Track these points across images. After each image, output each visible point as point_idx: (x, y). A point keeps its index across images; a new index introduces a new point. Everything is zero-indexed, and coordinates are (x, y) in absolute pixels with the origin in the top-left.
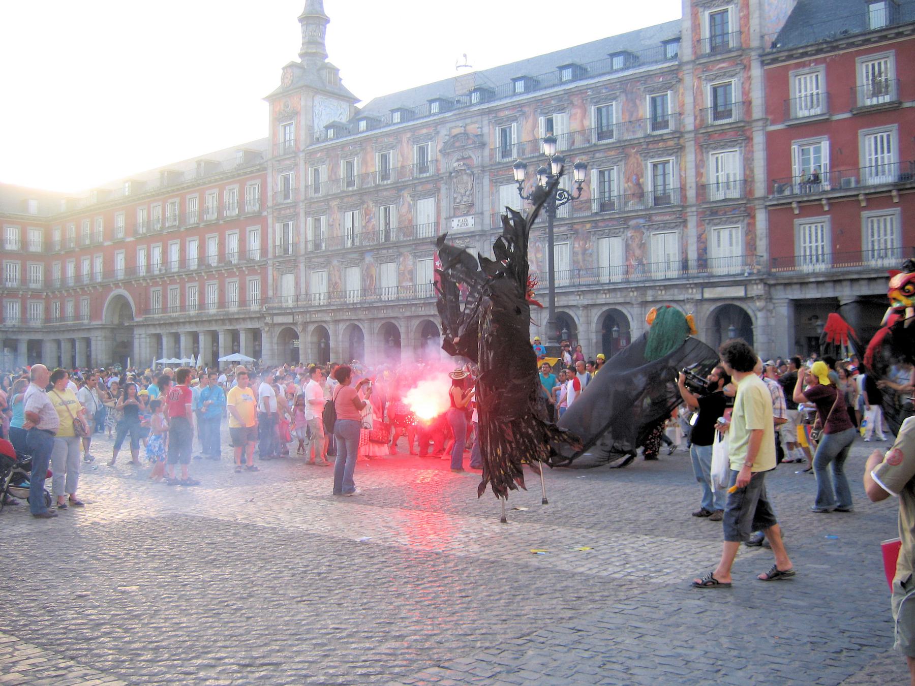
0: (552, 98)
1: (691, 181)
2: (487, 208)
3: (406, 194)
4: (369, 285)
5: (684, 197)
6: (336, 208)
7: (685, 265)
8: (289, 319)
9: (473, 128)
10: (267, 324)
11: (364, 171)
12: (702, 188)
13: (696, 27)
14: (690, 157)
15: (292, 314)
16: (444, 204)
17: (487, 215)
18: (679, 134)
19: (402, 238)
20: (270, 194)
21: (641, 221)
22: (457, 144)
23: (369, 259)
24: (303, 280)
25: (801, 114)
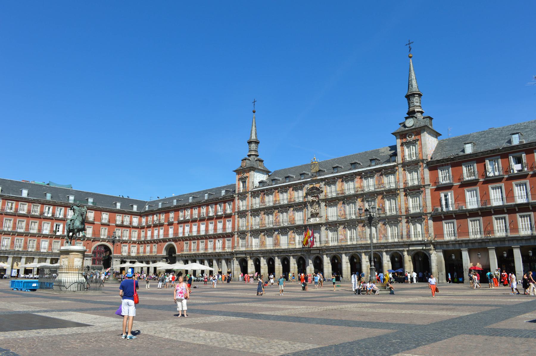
1: (403, 206)
3: (292, 209)
9: (317, 186)
12: (407, 210)
13: (403, 151)
20: (236, 207)
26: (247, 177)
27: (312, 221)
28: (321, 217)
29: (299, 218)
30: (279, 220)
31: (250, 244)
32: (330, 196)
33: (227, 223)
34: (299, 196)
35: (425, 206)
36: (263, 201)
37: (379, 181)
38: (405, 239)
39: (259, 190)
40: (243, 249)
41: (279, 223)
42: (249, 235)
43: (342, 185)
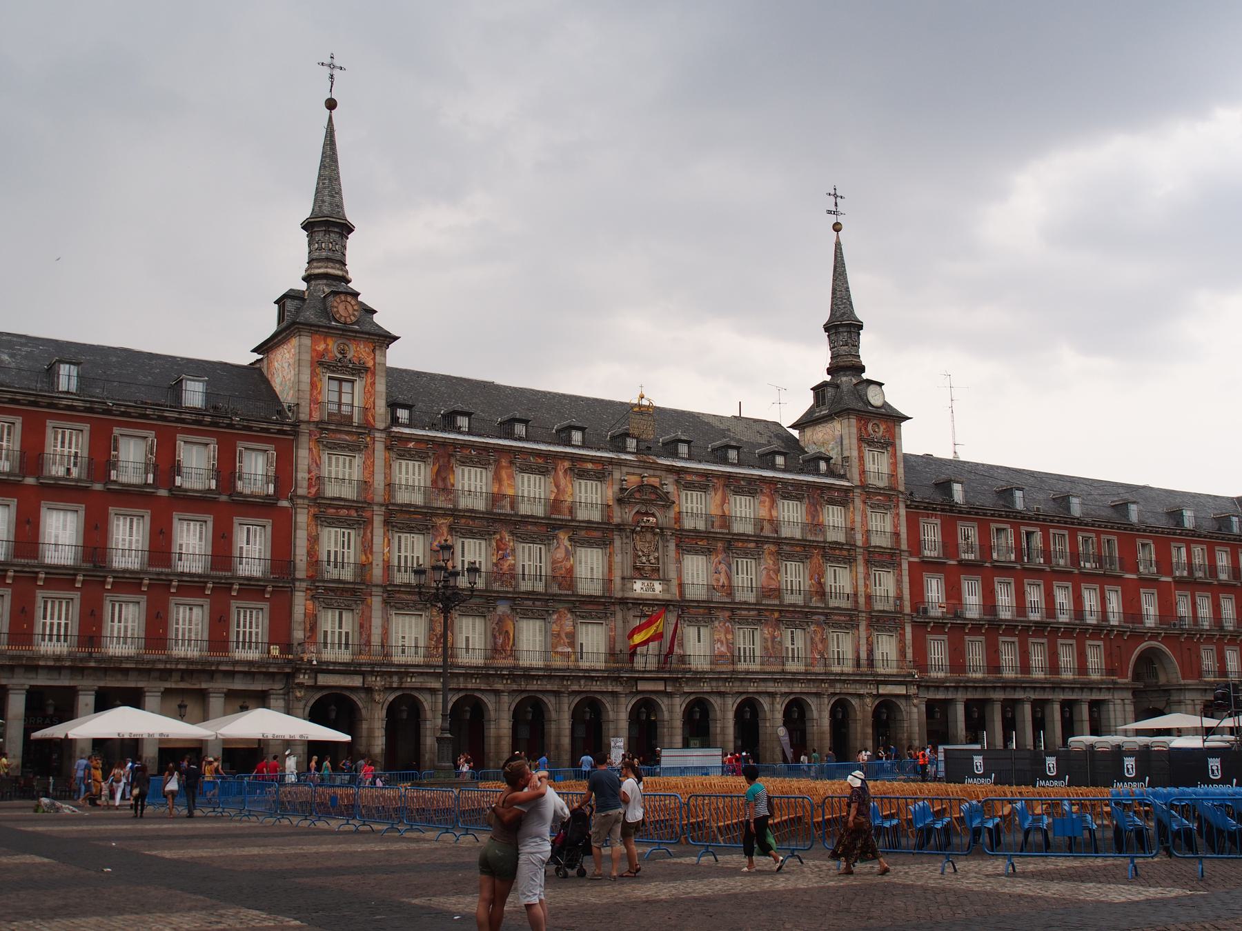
0: (743, 479)
2: (672, 575)
3: (563, 537)
4: (501, 643)
5: (856, 602)
6: (445, 530)
7: (858, 665)
8: (357, 681)
9: (654, 481)
10: (301, 686)
11: (496, 490)
12: (869, 598)
13: (861, 458)
14: (861, 569)
15: (363, 674)
16: (618, 559)
17: (675, 582)
18: (851, 545)
19: (555, 589)
20: (302, 475)
21: (822, 618)
22: (637, 495)
23: (503, 608)
24: (377, 622)
25: (927, 553)
26: (367, 369)
27: (639, 587)
28: (665, 580)
29: (590, 568)
30: (513, 567)
31: (376, 639)
32: (688, 524)
33: (240, 536)
34: (589, 499)
35: (899, 597)
36: (441, 482)
37: (813, 517)
38: (864, 669)
39: (432, 440)
40: (345, 656)
41: (513, 577)
42: (376, 602)
43: (723, 502)
